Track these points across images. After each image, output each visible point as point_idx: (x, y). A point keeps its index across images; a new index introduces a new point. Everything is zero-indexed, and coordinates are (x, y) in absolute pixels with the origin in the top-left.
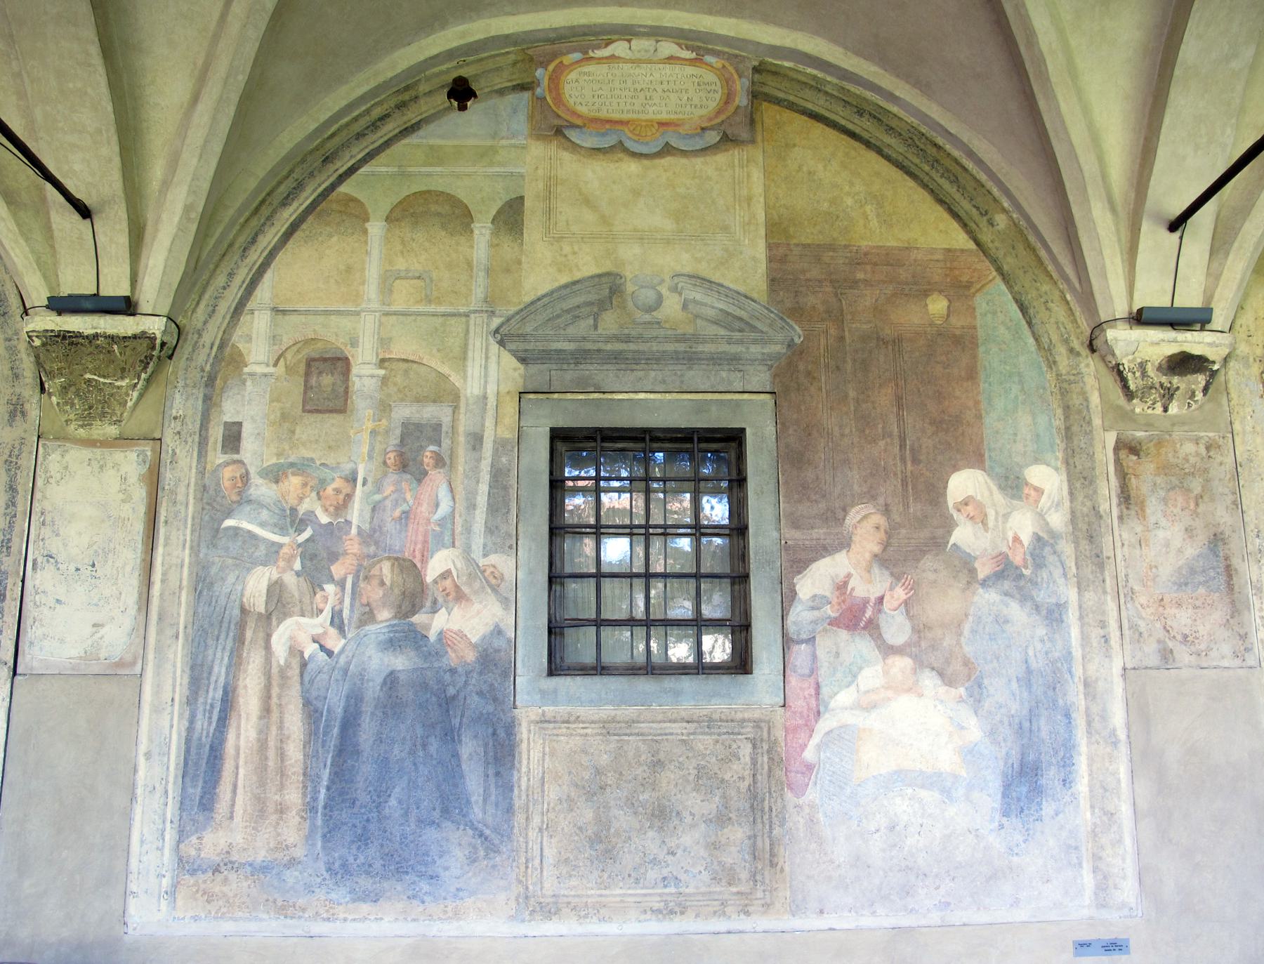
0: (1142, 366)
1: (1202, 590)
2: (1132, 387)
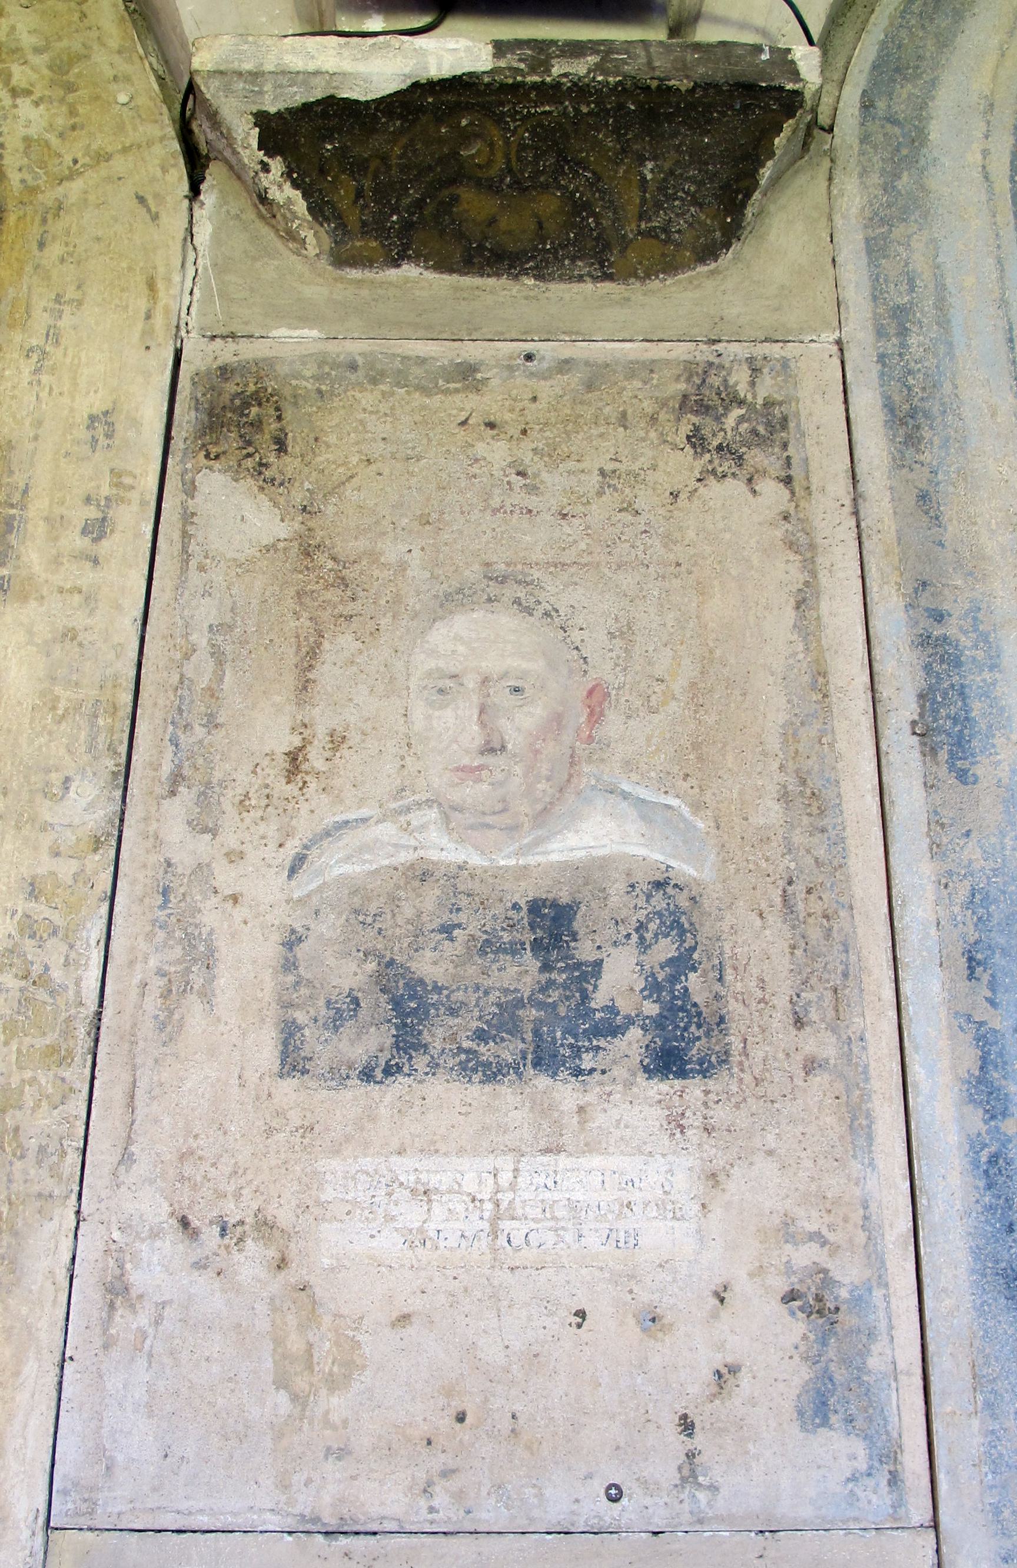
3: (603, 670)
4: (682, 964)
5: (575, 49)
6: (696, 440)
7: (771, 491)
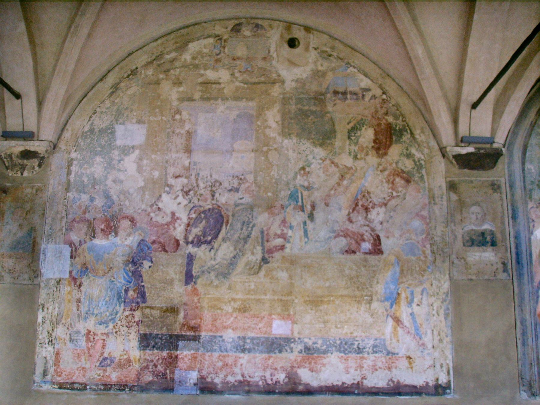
0: (10, 156)
1: (21, 251)
2: (7, 165)
3: (486, 212)
4: (493, 237)
5: (482, 149)
6: (492, 189)
7: (499, 194)
